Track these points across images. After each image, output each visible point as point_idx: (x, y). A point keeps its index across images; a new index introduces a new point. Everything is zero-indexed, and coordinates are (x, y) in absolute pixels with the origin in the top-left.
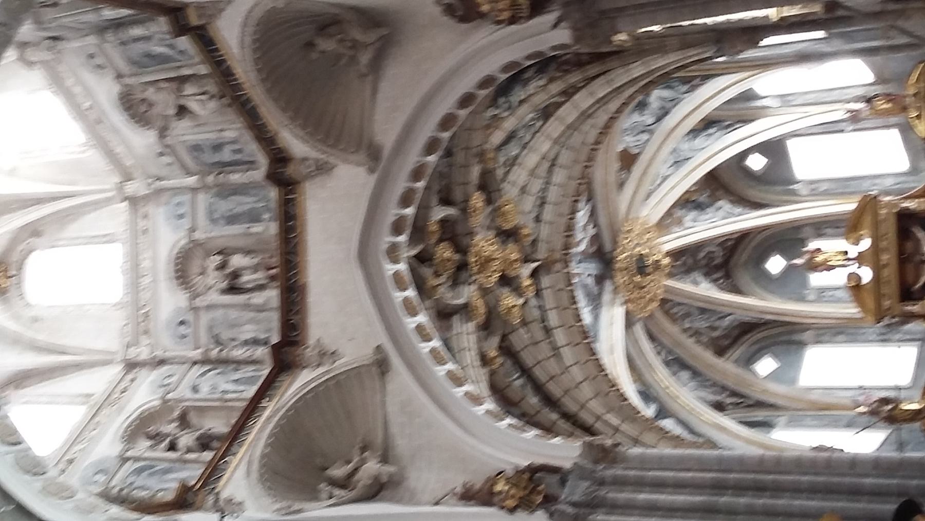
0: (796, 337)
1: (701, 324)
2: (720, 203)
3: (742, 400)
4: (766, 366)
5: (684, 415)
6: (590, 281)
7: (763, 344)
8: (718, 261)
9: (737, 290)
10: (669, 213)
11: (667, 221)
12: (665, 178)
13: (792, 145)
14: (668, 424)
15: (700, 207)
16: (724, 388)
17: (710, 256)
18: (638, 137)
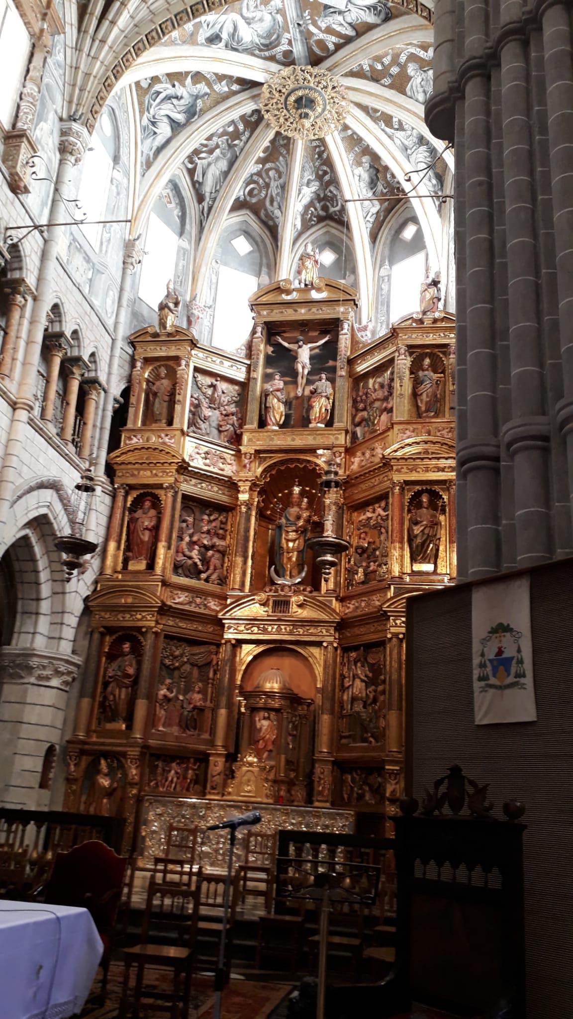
0: (264, 269)
1: (274, 190)
2: (376, 202)
3: (205, 215)
4: (243, 246)
5: (174, 144)
6: (284, 47)
7: (260, 243)
8: (332, 210)
9: (306, 225)
10: (367, 150)
11: (354, 141)
12: (390, 137)
13: (420, 257)
14: (164, 130)
15: (373, 184)
16: (214, 200)
17: (333, 199)
18: (421, 90)
